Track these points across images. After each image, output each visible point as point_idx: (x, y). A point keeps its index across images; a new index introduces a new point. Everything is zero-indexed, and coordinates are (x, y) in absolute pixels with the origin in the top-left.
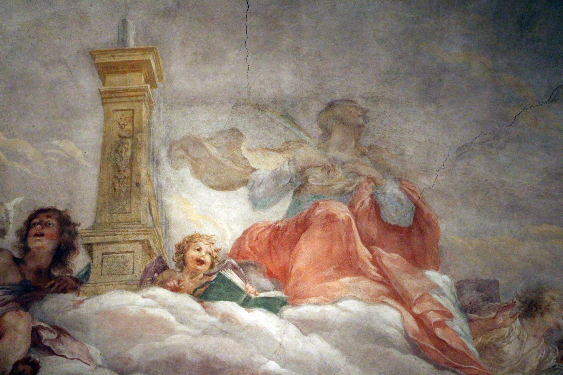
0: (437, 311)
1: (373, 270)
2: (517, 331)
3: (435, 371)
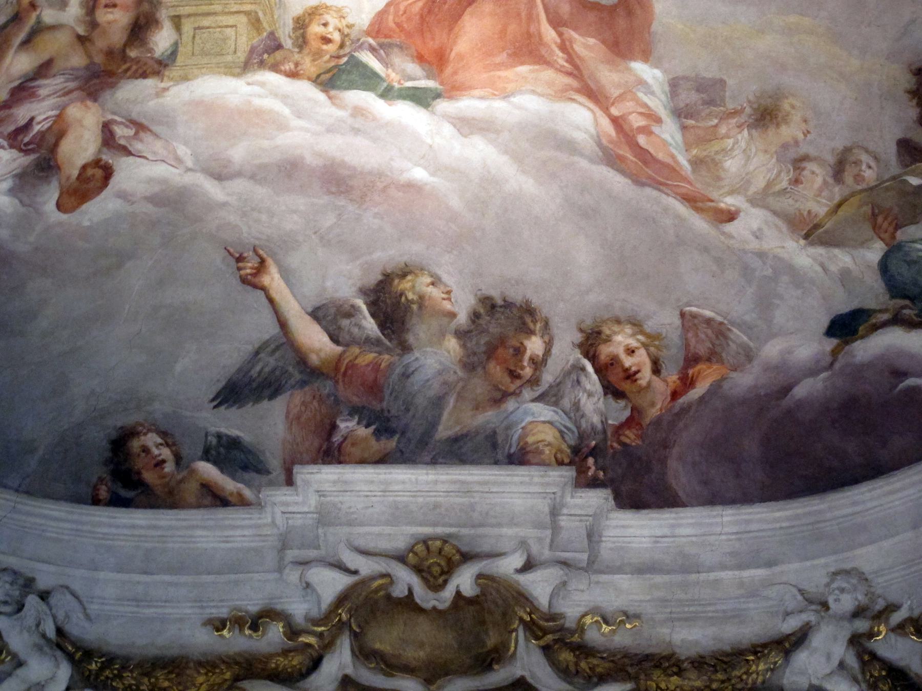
0: (641, 114)
1: (560, 58)
2: (743, 144)
3: (633, 187)
